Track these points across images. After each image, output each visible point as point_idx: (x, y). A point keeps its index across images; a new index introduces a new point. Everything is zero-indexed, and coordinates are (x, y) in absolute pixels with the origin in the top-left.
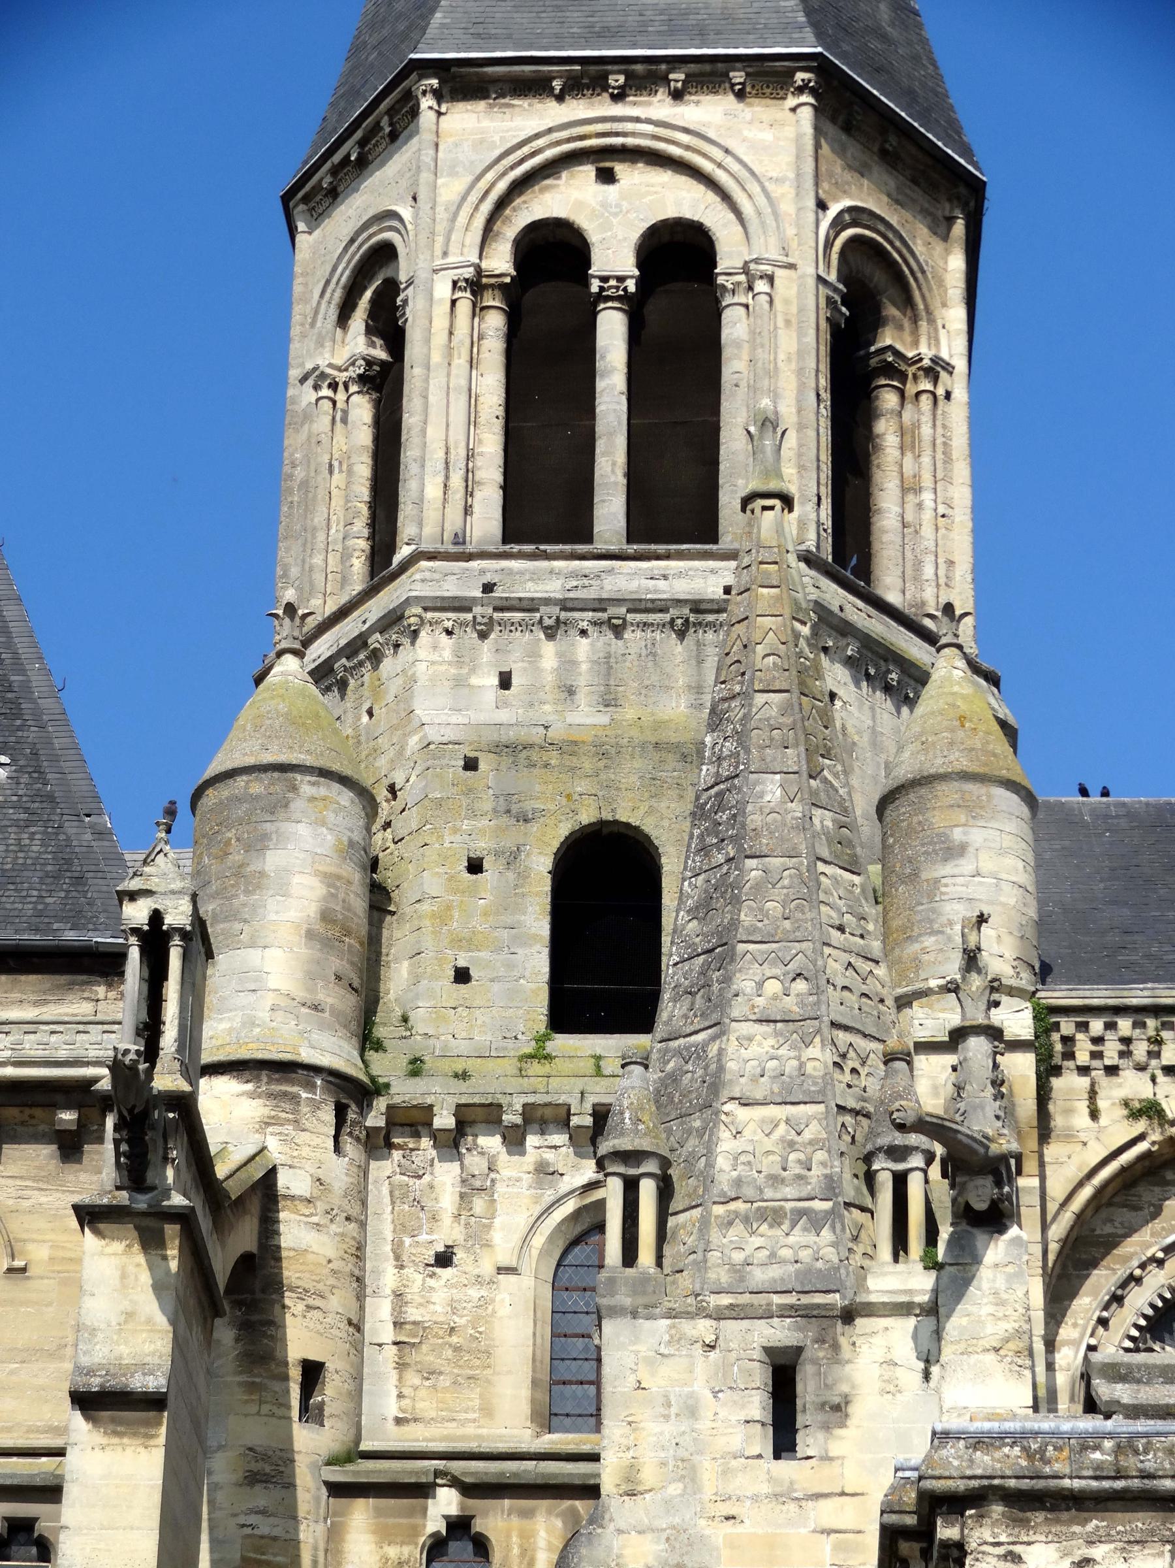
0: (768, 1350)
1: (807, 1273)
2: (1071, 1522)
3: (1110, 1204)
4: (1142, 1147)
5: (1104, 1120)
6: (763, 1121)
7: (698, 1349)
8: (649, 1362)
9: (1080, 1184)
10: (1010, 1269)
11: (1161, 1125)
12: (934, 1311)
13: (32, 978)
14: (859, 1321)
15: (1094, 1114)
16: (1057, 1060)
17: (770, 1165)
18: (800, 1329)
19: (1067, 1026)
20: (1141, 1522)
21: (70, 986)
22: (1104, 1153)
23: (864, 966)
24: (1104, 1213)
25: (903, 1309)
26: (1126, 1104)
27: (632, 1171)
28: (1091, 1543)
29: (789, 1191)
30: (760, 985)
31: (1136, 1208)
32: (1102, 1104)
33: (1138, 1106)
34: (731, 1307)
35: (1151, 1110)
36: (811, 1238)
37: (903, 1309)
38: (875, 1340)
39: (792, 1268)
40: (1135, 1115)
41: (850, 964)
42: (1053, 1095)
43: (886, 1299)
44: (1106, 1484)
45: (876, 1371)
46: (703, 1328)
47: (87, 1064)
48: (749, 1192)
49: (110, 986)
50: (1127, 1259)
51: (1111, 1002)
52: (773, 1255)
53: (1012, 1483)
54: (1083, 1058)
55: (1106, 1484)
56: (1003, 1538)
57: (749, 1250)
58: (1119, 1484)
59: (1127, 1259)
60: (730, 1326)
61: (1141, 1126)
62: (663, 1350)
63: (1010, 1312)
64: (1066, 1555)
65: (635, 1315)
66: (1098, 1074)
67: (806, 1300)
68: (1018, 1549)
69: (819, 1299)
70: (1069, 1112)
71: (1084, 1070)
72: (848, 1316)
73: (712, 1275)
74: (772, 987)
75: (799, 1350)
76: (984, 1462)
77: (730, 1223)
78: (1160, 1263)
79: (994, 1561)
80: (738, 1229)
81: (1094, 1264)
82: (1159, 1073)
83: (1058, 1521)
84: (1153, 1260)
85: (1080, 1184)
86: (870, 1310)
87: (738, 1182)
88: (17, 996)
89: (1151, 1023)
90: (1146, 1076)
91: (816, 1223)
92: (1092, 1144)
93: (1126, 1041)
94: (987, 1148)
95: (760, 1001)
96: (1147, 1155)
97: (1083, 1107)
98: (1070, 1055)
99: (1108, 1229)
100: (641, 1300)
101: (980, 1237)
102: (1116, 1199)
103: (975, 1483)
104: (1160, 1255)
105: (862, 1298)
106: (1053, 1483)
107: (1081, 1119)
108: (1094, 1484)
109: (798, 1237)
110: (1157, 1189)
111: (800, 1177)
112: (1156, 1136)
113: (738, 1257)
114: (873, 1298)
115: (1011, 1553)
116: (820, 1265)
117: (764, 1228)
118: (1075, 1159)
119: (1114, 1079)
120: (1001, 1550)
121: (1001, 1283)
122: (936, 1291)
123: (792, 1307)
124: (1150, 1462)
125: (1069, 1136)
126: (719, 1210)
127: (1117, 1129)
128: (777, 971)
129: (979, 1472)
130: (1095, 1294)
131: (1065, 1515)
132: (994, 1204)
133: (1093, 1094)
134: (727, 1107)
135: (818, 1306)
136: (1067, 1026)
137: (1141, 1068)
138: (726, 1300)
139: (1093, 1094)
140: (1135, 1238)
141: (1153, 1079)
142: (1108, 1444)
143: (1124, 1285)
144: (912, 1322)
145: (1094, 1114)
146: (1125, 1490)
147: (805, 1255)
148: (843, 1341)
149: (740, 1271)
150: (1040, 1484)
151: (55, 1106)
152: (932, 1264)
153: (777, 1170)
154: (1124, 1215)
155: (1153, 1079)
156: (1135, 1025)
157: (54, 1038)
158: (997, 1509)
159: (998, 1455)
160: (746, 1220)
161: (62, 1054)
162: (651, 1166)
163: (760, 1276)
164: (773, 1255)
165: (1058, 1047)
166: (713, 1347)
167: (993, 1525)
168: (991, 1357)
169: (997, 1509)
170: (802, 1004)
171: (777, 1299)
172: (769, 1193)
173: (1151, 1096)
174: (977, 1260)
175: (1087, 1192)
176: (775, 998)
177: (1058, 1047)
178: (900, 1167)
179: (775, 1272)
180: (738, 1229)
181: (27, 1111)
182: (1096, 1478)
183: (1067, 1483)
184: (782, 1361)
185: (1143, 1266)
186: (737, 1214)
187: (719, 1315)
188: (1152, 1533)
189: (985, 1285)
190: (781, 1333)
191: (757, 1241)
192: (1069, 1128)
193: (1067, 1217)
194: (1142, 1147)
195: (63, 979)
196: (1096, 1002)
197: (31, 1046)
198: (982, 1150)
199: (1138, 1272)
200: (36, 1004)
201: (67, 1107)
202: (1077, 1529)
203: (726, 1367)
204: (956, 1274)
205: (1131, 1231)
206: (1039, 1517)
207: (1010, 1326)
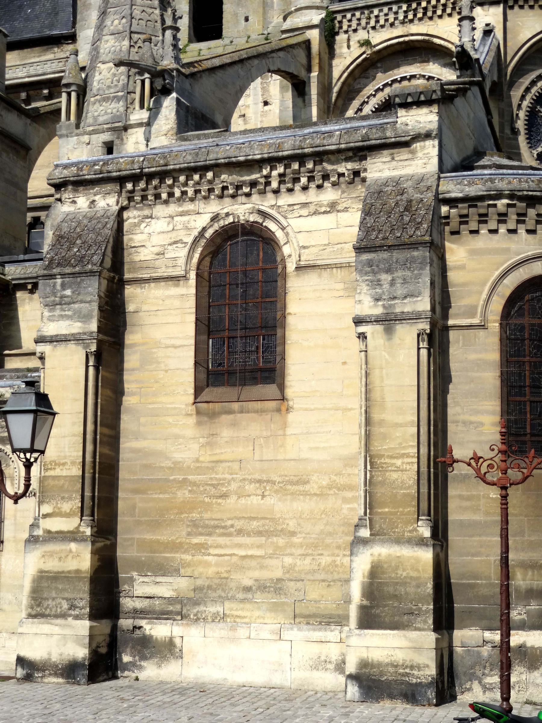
0: (104, 143)
1: (115, 116)
2: (89, 189)
3: (359, 77)
4: (364, 56)
5: (352, 49)
6: (108, 68)
7: (85, 145)
8: (71, 151)
9: (344, 72)
10: (170, 108)
11: (371, 48)
12: (149, 124)
13: (37, 48)
14: (129, 131)
15: (349, 47)
16: (337, 30)
17: (108, 83)
18: (113, 135)
19: (339, 17)
20: (109, 187)
21: (47, 50)
22: (351, 60)
23: (150, 11)
24: (357, 81)
25: (140, 125)
26: (359, 42)
27: (69, 90)
28: (95, 195)
29: (112, 90)
30: (113, 22)
31: (367, 78)
32: (351, 43)
33: (362, 42)
34: (93, 130)
35: (367, 43)
36: (117, 105)
37: (140, 125)
38: (134, 136)
39: (110, 116)
40: (362, 45)
41: (144, 11)
42: (336, 42)
43: (135, 122)
44: (97, 176)
45: (133, 146)
46: (86, 138)
47: (47, 74)
48: (101, 92)
49: (58, 47)
50: (364, 96)
51: (352, 7)
52: (106, 112)
53: (72, 179)
54: (345, 28)
55: (97, 176)
56: (71, 196)
57: (99, 111)
58: (101, 176)
59: (364, 96)
60: (94, 137)
61: (363, 49)
62: (75, 147)
63: (170, 122)
64: (88, 200)
65: (67, 136)
66: (351, 33)
67: (114, 125)
68: (75, 199)
69: (117, 125)
70: (341, 47)
71: (346, 32)
72: (126, 128)
73: (88, 121)
74: (116, 22)
75: (112, 142)
76: (66, 172)
77: (95, 103)
78: (374, 96)
79: (68, 203)
80: (97, 104)
81: (354, 99)
82: (370, 29)
83: (86, 189)
84: (371, 95)
85: (344, 72)
86: (132, 126)
87: (99, 90)
88: (33, 55)
89: (366, 12)
90: (366, 31)
91: (118, 99)
92: (348, 58)
93: (359, 20)
94: (156, 68)
95: (112, 28)
96: (366, 59)
97: (345, 45)
98: (341, 27)
99: (359, 86)
100: (69, 131)
101: (163, 98)
102: (362, 75)
103: (61, 180)
104: (374, 93)
105: (128, 123)
106: (83, 177)
107: (345, 50)
108: (94, 176)
109: (113, 105)
110: (375, 70)
111: (116, 85)
112: (369, 52)
113: (96, 114)
114: (132, 122)
115: (73, 201)
116: (118, 113)
117: (104, 103)
118: (342, 63)
119: (357, 34)
120: (71, 200)
121: (168, 113)
122: (149, 118)
123: (110, 128)
124: (110, 168)
125: (341, 56)
126: (92, 99)
127: (356, 51)
128: (118, 17)
129: (62, 176)
130: (353, 109)
131: (88, 187)
132: (164, 87)
133: (349, 40)
134: (99, 65)
135: (117, 127)
136: (339, 17)
137: (364, 28)
138: (91, 128)
139: (349, 40)
140: (367, 88)
141: (368, 32)
142: (101, 163)
143: (362, 105)
144: (144, 128)
145: (349, 47)
146: (102, 178)
147: (114, 111)
148: (124, 137)
149: (95, 118)
150: (79, 178)
151: (42, 89)
152: (149, 109)
153: (110, 84)
154: (363, 81)
155: (368, 32)
156: (361, 14)
157: (38, 67)
158: (70, 187)
159: (69, 170)
160: (99, 102)
161: (40, 72)
162: (73, 88)
163: (101, 119)
164: (106, 112)
165: (337, 25)
166: (89, 144)
167: (69, 192)
168: (164, 137)
169: (70, 187)
170: (123, 27)
171: (105, 126)
172: (107, 92)
173: (367, 38)
174: (161, 106)
175: (346, 74)
176: (116, 26)
177: (337, 25)
178: (143, 78)
179: (105, 117)
180: (97, 104)
181: (36, 91)
182: (95, 174)
183: (87, 177)
184: (109, 146)
185: (368, 97)
186: (97, 100)
187: (90, 133)
188: (112, 190)
189: (163, 114)
190: (106, 137)
191: (102, 108)
192: (341, 53)
193: (339, 84)
194: (364, 56)
195: (45, 47)
196: (347, 7)
197: (32, 71)
198: (154, 69)
199: (366, 100)
200: (39, 56)
201: (46, 89)
202: (91, 191)
203: (92, 150)
204: (155, 111)
205: (366, 85)
206: (81, 188)
207: (169, 126)
